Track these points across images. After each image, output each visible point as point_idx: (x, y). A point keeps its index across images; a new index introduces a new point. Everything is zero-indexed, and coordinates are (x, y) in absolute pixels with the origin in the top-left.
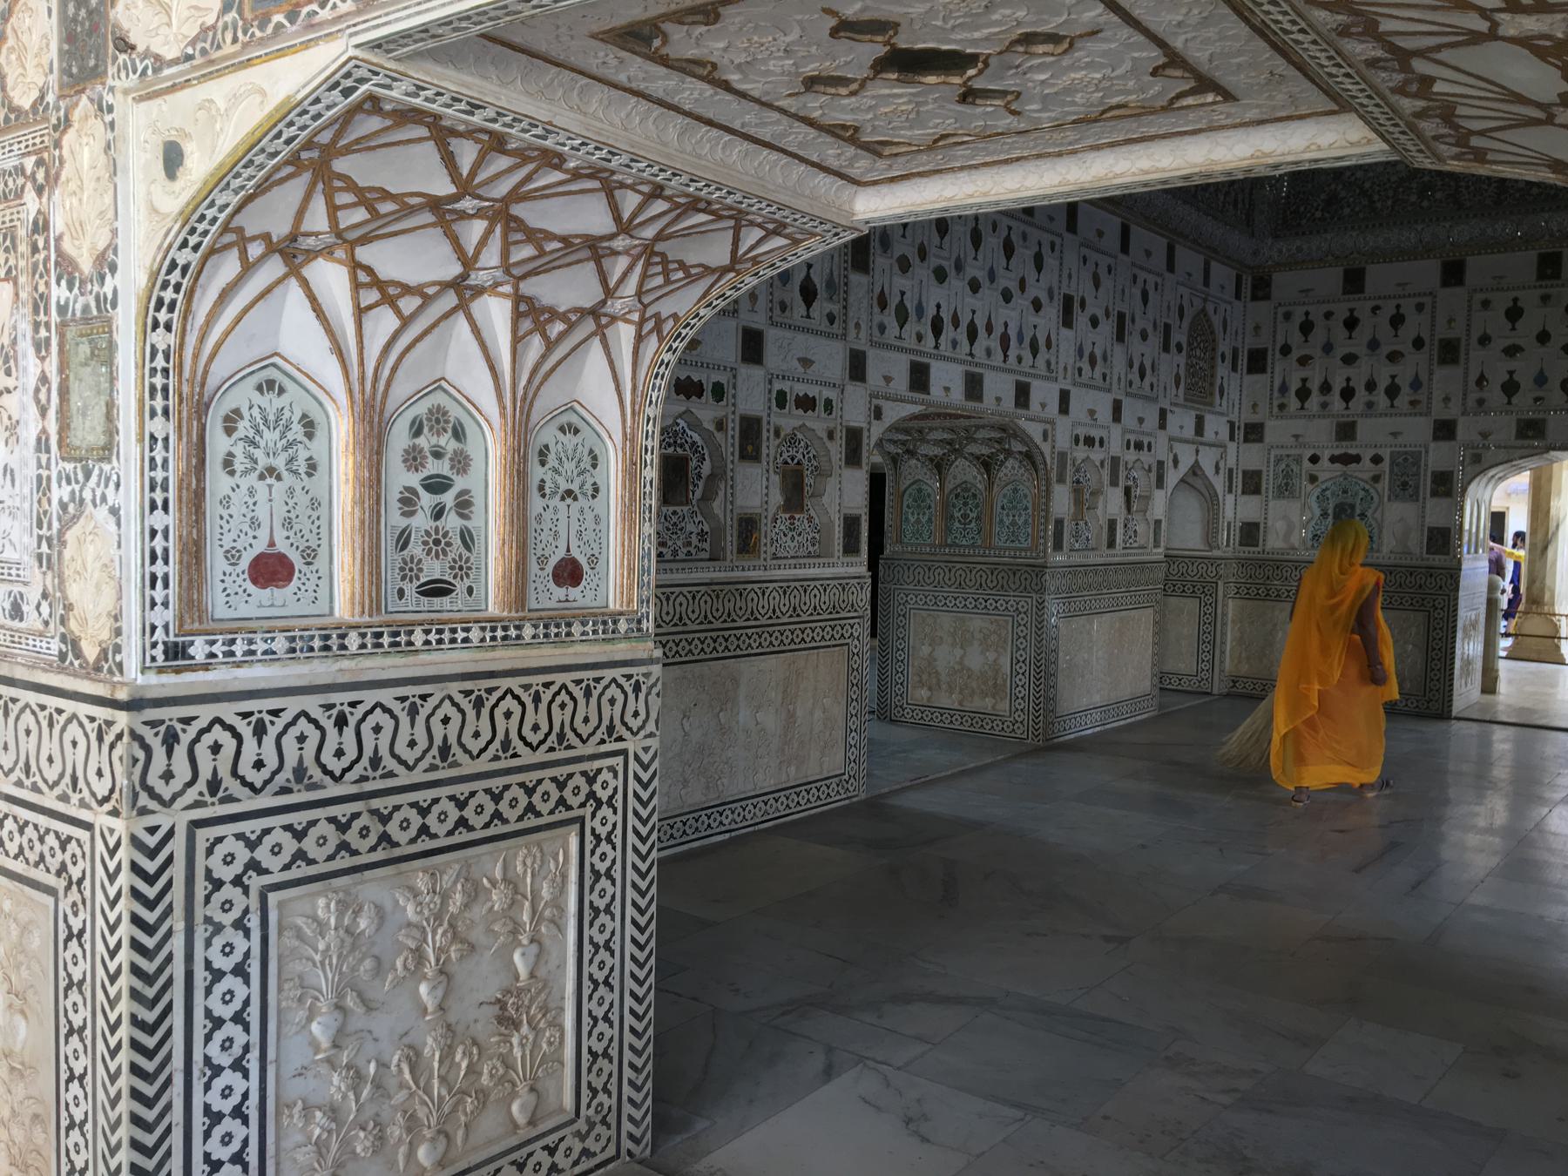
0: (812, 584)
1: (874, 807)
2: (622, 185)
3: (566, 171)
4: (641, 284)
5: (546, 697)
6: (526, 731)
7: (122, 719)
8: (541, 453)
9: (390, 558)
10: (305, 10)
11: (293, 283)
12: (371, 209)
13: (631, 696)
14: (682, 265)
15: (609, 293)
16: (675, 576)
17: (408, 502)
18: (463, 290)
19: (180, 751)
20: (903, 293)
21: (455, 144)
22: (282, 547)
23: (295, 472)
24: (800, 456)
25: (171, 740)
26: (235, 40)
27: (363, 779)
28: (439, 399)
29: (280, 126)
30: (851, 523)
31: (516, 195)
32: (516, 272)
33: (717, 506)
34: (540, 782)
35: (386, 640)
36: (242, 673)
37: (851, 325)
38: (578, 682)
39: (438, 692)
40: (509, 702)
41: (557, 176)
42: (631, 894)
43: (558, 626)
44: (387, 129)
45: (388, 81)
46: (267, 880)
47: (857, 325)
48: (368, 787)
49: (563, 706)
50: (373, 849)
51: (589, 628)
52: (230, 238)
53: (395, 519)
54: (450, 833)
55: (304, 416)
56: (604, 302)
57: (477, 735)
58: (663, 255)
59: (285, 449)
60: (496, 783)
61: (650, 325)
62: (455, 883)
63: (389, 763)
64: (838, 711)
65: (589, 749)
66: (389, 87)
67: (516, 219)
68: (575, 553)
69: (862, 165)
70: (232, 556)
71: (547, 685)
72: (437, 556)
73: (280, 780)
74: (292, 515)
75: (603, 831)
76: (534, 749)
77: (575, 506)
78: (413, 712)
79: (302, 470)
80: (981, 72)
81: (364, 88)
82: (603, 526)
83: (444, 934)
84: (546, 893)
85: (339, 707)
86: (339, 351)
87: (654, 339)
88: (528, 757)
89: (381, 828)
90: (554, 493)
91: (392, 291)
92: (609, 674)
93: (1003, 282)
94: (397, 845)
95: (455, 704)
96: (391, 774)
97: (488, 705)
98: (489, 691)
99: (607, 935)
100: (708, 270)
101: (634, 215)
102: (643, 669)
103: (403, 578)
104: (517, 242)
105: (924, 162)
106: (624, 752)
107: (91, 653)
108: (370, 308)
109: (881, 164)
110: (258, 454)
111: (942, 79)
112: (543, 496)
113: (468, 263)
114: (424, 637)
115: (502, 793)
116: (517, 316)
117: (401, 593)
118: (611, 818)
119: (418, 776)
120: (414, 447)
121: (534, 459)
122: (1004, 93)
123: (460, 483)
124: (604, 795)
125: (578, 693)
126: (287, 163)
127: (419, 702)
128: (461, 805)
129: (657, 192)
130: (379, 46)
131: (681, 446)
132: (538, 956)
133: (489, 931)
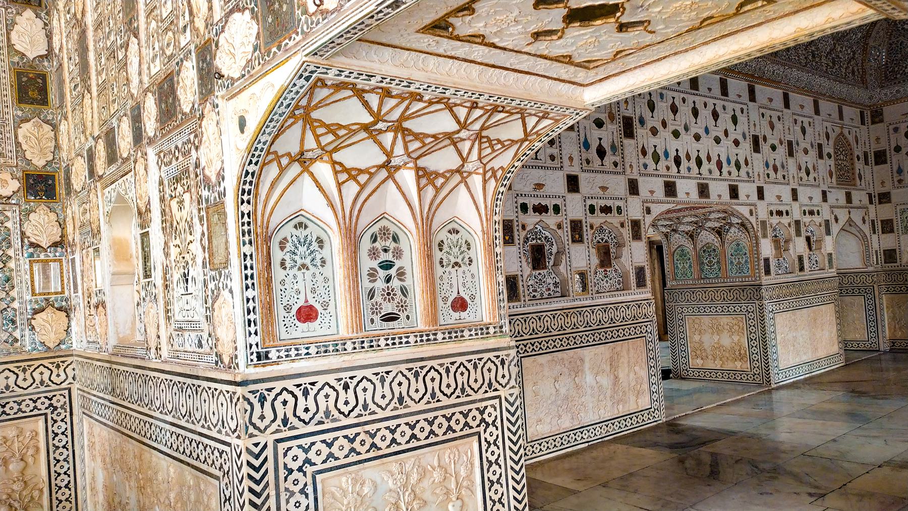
0: (620, 305)
1: (672, 426)
2: (456, 105)
3: (425, 102)
4: (480, 154)
5: (453, 370)
6: (444, 388)
7: (240, 390)
8: (439, 245)
9: (366, 304)
10: (283, 44)
11: (306, 175)
12: (335, 134)
13: (500, 367)
14: (499, 141)
15: (464, 160)
16: (542, 307)
17: (372, 275)
19: (267, 405)
20: (655, 146)
21: (367, 96)
22: (311, 302)
23: (315, 265)
24: (606, 238)
25: (262, 400)
26: (259, 64)
27: (360, 415)
29: (281, 100)
30: (640, 272)
31: (403, 118)
32: (414, 155)
33: (562, 268)
34: (453, 414)
35: (366, 345)
36: (294, 365)
37: (627, 166)
38: (469, 361)
39: (395, 369)
40: (433, 373)
41: (421, 105)
42: (511, 473)
43: (456, 332)
44: (332, 94)
45: (325, 70)
46: (315, 468)
47: (631, 166)
48: (362, 419)
49: (462, 374)
50: (368, 451)
51: (473, 332)
52: (271, 157)
53: (367, 284)
54: (408, 442)
55: (318, 238)
56: (463, 166)
57: (417, 391)
58: (487, 137)
59: (310, 254)
60: (430, 416)
61: (489, 174)
62: (413, 468)
64: (644, 373)
65: (479, 396)
66: (326, 73)
67: (407, 129)
68: (462, 294)
69: (581, 75)
70: (288, 308)
72: (389, 301)
77: (460, 270)
78: (383, 380)
79: (319, 264)
80: (623, 13)
81: (314, 75)
82: (476, 279)
83: (410, 494)
84: (463, 473)
85: (344, 380)
86: (331, 205)
87: (493, 181)
88: (445, 401)
91: (353, 173)
92: (486, 356)
93: (694, 130)
94: (380, 449)
96: (374, 413)
97: (422, 375)
98: (422, 368)
99: (499, 495)
100: (513, 142)
101: (466, 119)
102: (505, 352)
103: (373, 313)
104: (411, 141)
105: (612, 68)
106: (499, 397)
107: (226, 360)
108: (344, 182)
109: (592, 73)
110: (297, 258)
111: (604, 21)
112: (443, 266)
113: (389, 154)
114: (385, 342)
116: (418, 177)
117: (372, 321)
118: (495, 433)
119: (388, 413)
120: (373, 248)
121: (435, 248)
122: (641, 23)
123: (398, 264)
124: (490, 420)
126: (289, 117)
127: (385, 375)
128: (412, 427)
129: (474, 106)
130: (316, 54)
131: (540, 239)
132: (462, 507)
133: (433, 493)
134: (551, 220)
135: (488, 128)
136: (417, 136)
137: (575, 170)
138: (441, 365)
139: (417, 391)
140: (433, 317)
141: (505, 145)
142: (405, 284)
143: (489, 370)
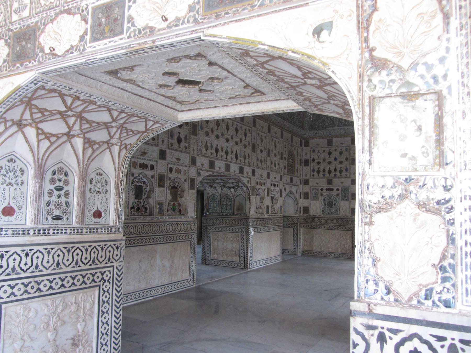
0: (180, 223)
1: (198, 289)
3: (97, 105)
5: (89, 249)
6: (83, 259)
8: (91, 181)
9: (44, 209)
10: (25, 64)
11: (20, 133)
13: (116, 250)
14: (132, 131)
15: (111, 137)
17: (50, 193)
18: (69, 136)
21: (66, 98)
22: (12, 205)
23: (17, 184)
26: (6, 70)
27: (33, 272)
28: (61, 165)
29: (17, 92)
31: (83, 111)
32: (84, 131)
34: (87, 274)
35: (42, 232)
38: (99, 246)
39: (57, 247)
40: (78, 251)
41: (95, 107)
42: (114, 308)
43: (94, 229)
44: (46, 94)
50: (35, 292)
51: (103, 230)
53: (47, 198)
54: (59, 288)
55: (21, 169)
56: (110, 140)
57: (68, 260)
58: (126, 128)
59: (15, 178)
60: (73, 274)
61: (123, 146)
62: (60, 303)
63: (41, 267)
65: (102, 265)
66: (47, 83)
67: (83, 117)
68: (100, 209)
69: (178, 107)
71: (90, 246)
72: (58, 209)
73: (7, 271)
74: (16, 196)
75: (106, 289)
76: (85, 265)
77: (100, 196)
78: (49, 253)
79: (19, 184)
80: (202, 85)
81: (40, 83)
82: (108, 201)
83: (56, 318)
84: (88, 307)
86: (32, 151)
87: (124, 150)
88: (83, 267)
89: (38, 287)
90: (94, 192)
91: (48, 135)
92: (109, 244)
94: (42, 291)
95: (61, 251)
96: (41, 271)
97: (72, 252)
98: (72, 247)
99: (107, 320)
100: (139, 132)
102: (119, 242)
103: (48, 215)
104: (84, 123)
105: (194, 106)
106: (113, 266)
108: (42, 140)
109: (183, 106)
110: (7, 179)
112: (91, 192)
113: (70, 128)
114: (53, 231)
115: (75, 277)
116: (84, 143)
117: (47, 219)
118: (109, 286)
119: (49, 271)
120: (53, 178)
121: (88, 182)
122: (210, 91)
123: (66, 188)
124: (106, 279)
125: (99, 249)
126: (19, 101)
127: (51, 250)
128: (62, 280)
129: (122, 112)
130: (44, 73)
131: (141, 182)
132: (85, 325)
133: (70, 317)
134: (149, 173)
135: (127, 123)
136: (88, 122)
137: (164, 147)
138: (83, 247)
139: (68, 260)
140: (82, 220)
141: (134, 133)
142: (68, 200)
143: (110, 251)
